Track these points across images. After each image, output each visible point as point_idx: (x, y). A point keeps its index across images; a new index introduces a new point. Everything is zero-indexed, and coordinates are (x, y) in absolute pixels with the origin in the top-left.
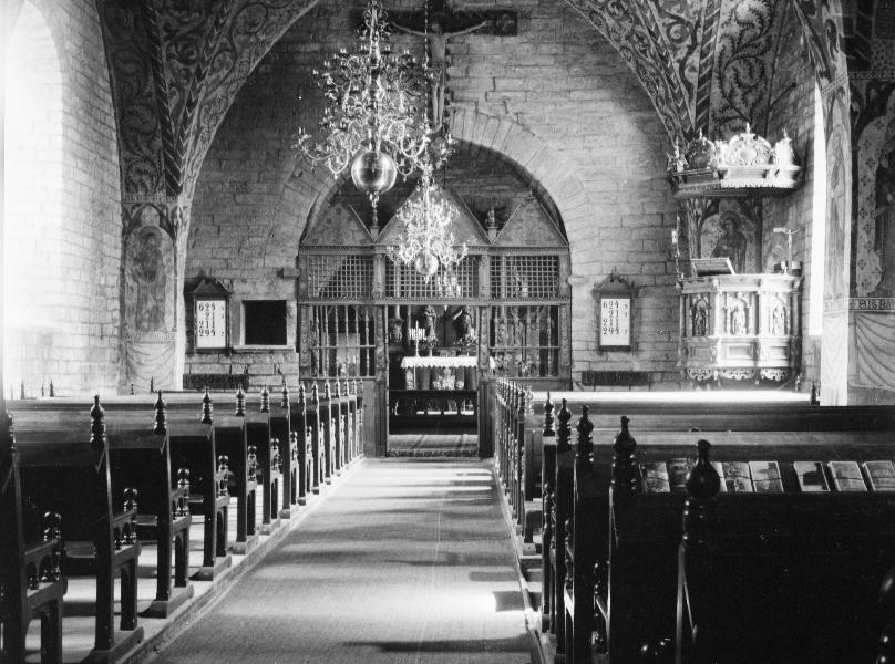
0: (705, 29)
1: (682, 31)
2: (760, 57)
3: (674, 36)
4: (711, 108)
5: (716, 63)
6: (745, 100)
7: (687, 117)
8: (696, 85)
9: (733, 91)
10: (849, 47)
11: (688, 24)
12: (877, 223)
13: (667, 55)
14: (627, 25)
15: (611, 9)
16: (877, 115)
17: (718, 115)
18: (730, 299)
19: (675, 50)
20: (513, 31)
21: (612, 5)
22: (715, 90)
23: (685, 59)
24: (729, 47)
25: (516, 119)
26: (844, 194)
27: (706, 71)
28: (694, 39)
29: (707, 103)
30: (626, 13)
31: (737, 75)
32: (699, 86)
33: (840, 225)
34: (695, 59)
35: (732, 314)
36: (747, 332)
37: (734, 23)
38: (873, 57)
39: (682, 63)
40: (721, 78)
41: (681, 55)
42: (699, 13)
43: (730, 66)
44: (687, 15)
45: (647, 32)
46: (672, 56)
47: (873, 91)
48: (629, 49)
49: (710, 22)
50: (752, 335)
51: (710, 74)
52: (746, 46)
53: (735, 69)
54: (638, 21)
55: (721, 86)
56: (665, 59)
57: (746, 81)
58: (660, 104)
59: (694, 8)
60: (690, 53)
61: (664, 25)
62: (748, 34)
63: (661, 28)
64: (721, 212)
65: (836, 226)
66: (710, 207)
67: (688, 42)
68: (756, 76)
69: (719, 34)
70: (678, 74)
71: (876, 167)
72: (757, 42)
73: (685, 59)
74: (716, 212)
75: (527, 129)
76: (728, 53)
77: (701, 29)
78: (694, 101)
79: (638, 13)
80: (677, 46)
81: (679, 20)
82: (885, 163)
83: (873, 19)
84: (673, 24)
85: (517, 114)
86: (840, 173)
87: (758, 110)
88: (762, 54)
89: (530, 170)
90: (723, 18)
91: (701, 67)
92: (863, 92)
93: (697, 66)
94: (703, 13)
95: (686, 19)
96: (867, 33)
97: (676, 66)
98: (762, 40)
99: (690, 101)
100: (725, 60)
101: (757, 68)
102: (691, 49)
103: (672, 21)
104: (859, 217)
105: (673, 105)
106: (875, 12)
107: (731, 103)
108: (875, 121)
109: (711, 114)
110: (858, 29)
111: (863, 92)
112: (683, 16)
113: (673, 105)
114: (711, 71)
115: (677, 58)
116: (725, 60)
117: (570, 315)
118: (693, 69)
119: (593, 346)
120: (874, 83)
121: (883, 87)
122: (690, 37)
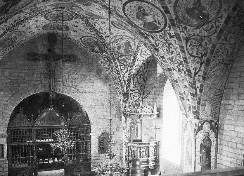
0: (130, 67)
1: (124, 68)
3: (122, 69)
4: (130, 87)
5: (132, 76)
6: (139, 85)
7: (124, 90)
8: (127, 81)
10: (194, 113)
11: (126, 66)
12: (200, 158)
13: (119, 73)
14: (108, 63)
15: (104, 58)
16: (200, 130)
17: (132, 89)
18: (142, 148)
19: (122, 72)
20: (74, 61)
21: (104, 57)
23: (124, 74)
24: (136, 72)
25: (75, 87)
26: (191, 148)
28: (127, 70)
29: (129, 86)
30: (108, 60)
31: (137, 79)
33: (190, 156)
34: (127, 74)
35: (142, 153)
36: (146, 157)
37: (138, 66)
38: (200, 115)
39: (123, 75)
40: (133, 80)
41: (123, 73)
42: (129, 63)
43: (136, 77)
44: (126, 63)
45: (114, 67)
46: (121, 73)
47: (200, 124)
48: (108, 68)
49: (132, 66)
50: (147, 158)
54: (111, 63)
56: (119, 74)
58: (116, 84)
59: (128, 62)
60: (126, 73)
61: (119, 65)
62: (141, 69)
63: (118, 66)
65: (188, 155)
67: (126, 70)
68: (142, 79)
69: (134, 69)
70: (122, 79)
71: (200, 143)
73: (124, 74)
75: (78, 90)
77: (129, 67)
79: (112, 61)
80: (122, 71)
81: (123, 64)
82: (202, 142)
83: (200, 106)
84: (122, 65)
85: (76, 86)
86: (190, 142)
87: (142, 88)
88: (144, 74)
89: (79, 102)
90: (135, 65)
92: (197, 124)
93: (127, 77)
94: (130, 64)
95: (126, 64)
96: (199, 110)
97: (122, 76)
98: (145, 71)
100: (135, 75)
101: (142, 77)
102: (126, 72)
103: (122, 64)
104: (196, 156)
105: (120, 85)
106: (201, 104)
107: (135, 86)
108: (200, 131)
109: (130, 89)
110: (197, 109)
111: (197, 124)
112: (125, 64)
114: (131, 78)
115: (122, 74)
116: (135, 75)
117: (90, 144)
119: (97, 152)
120: (200, 122)
121: (202, 123)
122: (126, 69)
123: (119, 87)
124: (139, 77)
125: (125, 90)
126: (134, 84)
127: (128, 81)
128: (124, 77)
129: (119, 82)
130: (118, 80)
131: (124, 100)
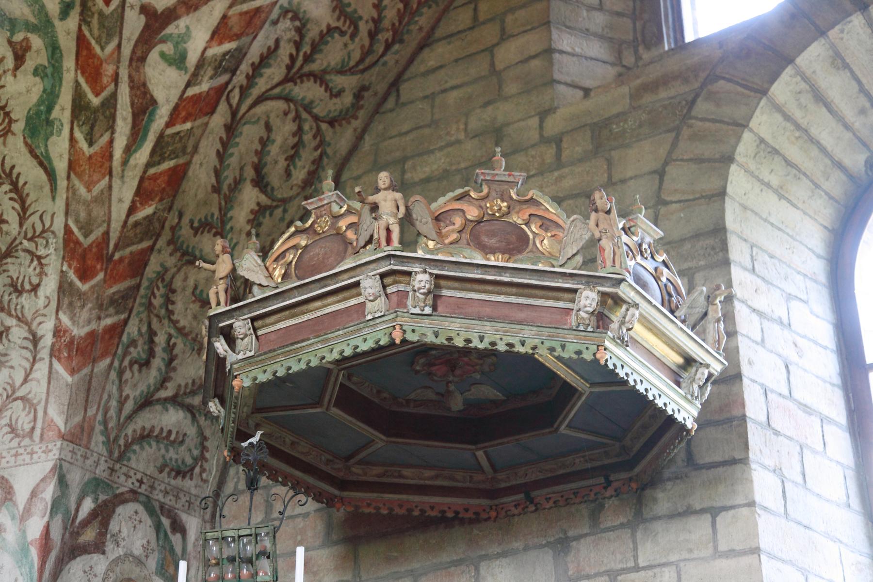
2: (324, 126)
8: (163, 113)
9: (238, 183)
17: (185, 231)
22: (208, 149)
24: (286, 50)
27: (204, 86)
29: (178, 176)
31: (264, 142)
32: (174, 118)
40: (231, 129)
43: (260, 110)
51: (204, 106)
52: (311, 75)
53: (268, 127)
55: (221, 156)
57: (275, 176)
64: (113, 552)
66: (86, 523)
72: (338, 81)
74: (98, 547)
76: (275, 72)
78: (142, 155)
91: (201, 64)
93: (193, 58)
99: (129, 151)
100: (261, 85)
107: (224, 212)
113: (59, 149)
114: (220, 92)
116: (261, 85)
118: (178, 61)
123: (30, 173)
124: (284, 131)
125: (119, 212)
126: (216, 189)
127: (190, 108)
128: (154, 56)
129: (65, 99)
130: (50, 73)
131: (79, 332)
